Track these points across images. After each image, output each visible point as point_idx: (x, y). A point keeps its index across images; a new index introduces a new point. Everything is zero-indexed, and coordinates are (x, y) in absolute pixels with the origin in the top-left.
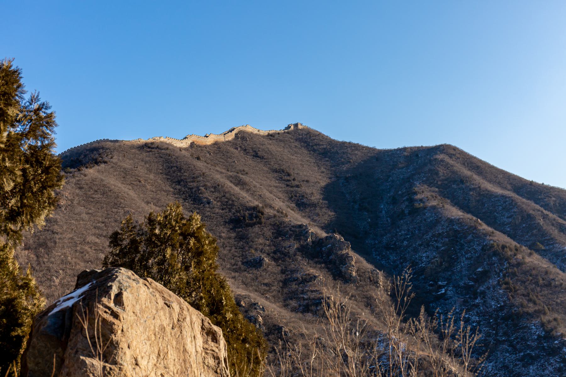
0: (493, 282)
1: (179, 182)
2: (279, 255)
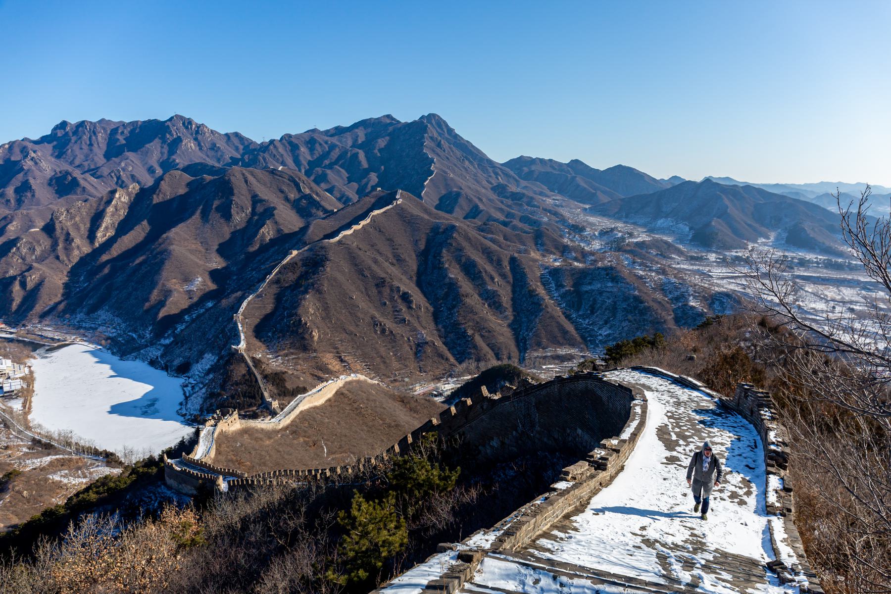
0: (455, 310)
1: (356, 265)
2: (392, 299)
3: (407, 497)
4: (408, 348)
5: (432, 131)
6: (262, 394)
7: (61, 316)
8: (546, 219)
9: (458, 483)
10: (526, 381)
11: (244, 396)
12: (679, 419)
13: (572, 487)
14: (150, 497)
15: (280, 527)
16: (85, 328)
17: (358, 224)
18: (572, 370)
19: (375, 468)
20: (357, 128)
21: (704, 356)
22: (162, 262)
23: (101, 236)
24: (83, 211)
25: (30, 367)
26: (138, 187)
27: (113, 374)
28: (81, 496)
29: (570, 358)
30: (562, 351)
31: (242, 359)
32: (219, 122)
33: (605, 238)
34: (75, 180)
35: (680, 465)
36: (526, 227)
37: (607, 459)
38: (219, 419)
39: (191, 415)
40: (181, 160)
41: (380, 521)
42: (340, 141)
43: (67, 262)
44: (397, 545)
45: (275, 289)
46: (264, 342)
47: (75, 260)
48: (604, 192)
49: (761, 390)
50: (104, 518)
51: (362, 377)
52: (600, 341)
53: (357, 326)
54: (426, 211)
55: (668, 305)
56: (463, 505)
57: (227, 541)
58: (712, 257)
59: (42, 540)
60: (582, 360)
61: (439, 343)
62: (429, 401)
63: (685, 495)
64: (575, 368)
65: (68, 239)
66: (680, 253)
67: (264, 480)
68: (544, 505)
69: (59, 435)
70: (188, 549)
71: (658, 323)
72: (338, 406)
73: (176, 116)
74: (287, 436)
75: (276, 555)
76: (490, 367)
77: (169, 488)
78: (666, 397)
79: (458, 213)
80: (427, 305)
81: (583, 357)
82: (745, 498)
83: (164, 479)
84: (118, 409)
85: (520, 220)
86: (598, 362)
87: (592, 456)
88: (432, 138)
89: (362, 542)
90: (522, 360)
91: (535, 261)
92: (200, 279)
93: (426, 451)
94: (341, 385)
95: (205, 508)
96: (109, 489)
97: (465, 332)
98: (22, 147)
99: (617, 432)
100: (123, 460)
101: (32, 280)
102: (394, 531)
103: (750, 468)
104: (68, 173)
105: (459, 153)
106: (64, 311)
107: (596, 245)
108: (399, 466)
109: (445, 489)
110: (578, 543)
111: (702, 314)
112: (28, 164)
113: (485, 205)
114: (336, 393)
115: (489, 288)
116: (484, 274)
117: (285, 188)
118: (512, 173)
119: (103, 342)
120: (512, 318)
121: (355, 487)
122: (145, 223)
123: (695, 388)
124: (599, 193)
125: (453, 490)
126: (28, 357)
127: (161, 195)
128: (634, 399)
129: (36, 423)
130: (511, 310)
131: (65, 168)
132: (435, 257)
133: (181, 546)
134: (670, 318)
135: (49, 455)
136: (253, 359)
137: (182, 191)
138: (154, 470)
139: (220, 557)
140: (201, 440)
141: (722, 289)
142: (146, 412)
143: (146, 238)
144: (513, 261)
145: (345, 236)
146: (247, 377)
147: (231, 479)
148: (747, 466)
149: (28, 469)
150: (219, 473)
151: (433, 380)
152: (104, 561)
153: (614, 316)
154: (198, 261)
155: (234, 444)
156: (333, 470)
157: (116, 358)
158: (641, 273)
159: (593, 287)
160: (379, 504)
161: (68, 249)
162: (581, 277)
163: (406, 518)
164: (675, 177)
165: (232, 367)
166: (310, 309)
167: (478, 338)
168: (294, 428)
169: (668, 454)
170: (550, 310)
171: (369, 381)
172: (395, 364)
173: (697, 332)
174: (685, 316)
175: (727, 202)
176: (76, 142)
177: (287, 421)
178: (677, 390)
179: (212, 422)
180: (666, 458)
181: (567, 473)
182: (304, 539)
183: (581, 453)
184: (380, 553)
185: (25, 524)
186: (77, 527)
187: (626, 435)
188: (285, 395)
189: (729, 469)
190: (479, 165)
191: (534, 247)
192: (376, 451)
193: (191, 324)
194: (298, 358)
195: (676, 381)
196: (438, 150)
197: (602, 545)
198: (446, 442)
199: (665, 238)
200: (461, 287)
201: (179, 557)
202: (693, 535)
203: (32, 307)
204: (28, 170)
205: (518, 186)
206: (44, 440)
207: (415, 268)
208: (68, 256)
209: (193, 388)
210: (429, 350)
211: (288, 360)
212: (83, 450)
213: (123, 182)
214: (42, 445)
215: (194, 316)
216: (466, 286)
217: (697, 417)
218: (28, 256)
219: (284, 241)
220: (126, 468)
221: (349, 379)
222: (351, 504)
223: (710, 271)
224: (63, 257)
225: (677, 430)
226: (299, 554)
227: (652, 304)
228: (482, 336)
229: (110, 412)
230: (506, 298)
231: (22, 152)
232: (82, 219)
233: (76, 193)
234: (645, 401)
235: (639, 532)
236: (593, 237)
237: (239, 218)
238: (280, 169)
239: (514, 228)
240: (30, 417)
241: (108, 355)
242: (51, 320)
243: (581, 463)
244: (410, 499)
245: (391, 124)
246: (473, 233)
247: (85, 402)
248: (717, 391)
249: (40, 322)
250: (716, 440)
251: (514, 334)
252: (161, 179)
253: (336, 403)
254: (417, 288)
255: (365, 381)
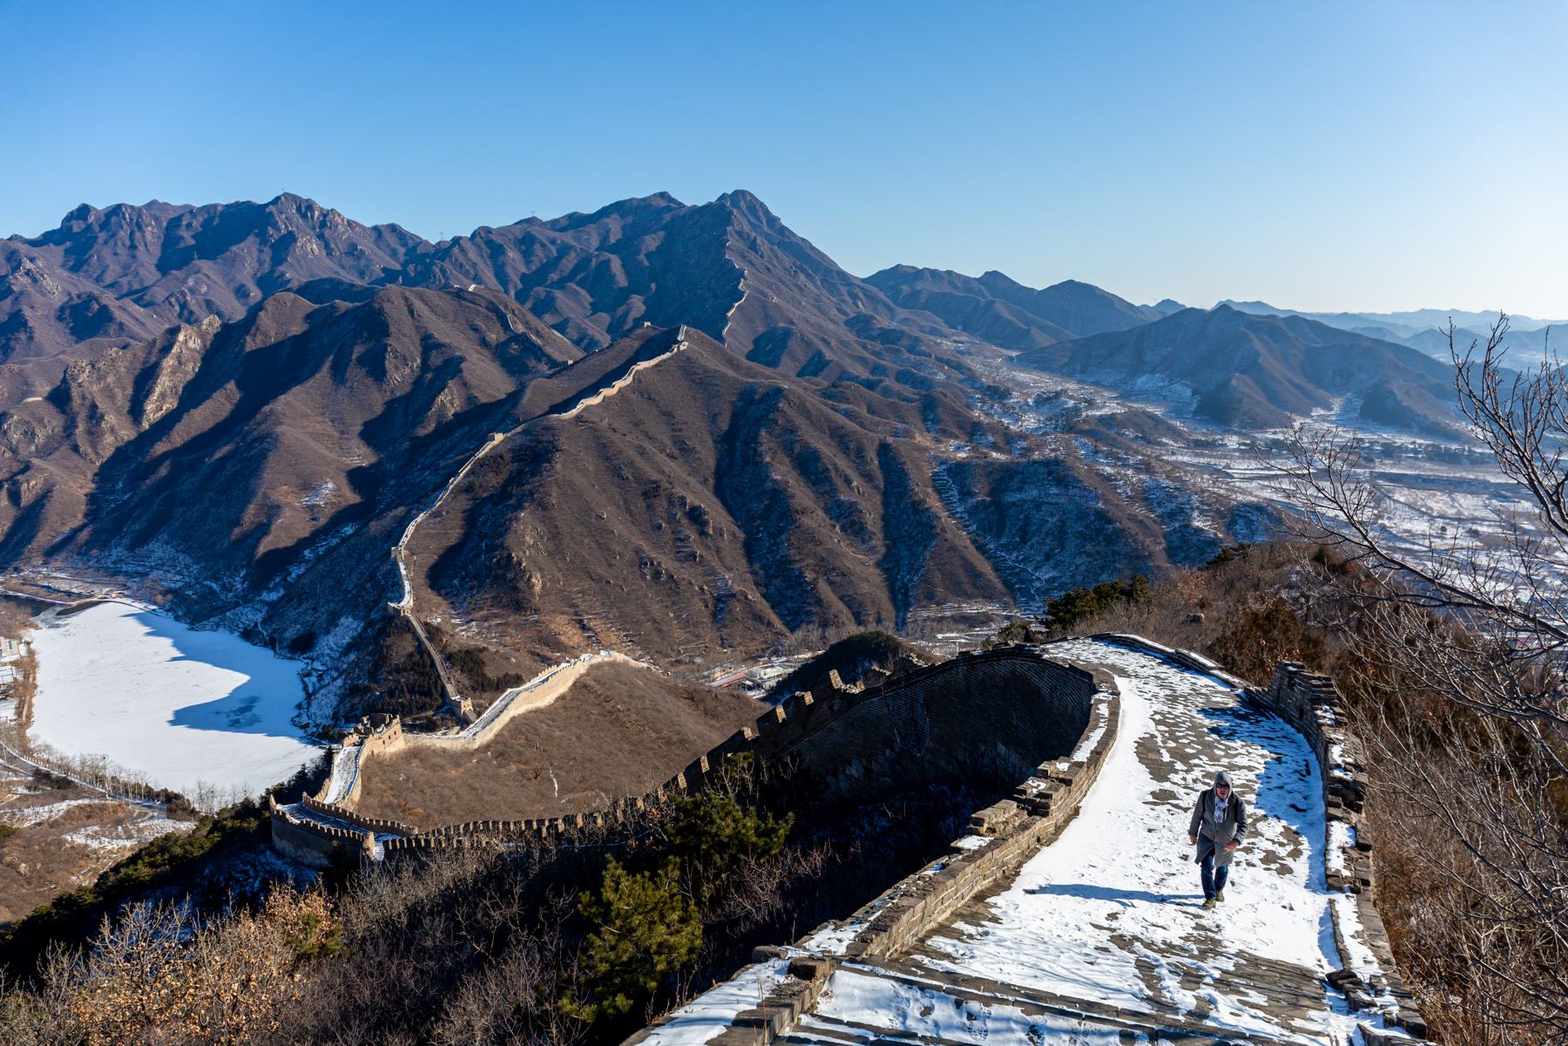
0: (783, 537)
2: (671, 518)
3: (700, 867)
4: (700, 605)
5: (741, 221)
6: (443, 688)
7: (83, 551)
8: (941, 377)
9: (790, 841)
10: (907, 661)
11: (412, 692)
12: (1176, 725)
13: (989, 845)
14: (246, 872)
15: (477, 921)
16: (126, 573)
17: (609, 385)
18: (988, 641)
19: (643, 815)
20: (608, 215)
21: (1218, 615)
22: (263, 456)
23: (153, 410)
24: (120, 365)
25: (28, 643)
26: (217, 322)
27: (178, 654)
28: (123, 870)
29: (984, 620)
30: (971, 609)
31: (407, 626)
32: (362, 207)
33: (1045, 409)
34: (104, 309)
35: (1177, 806)
36: (907, 391)
37: (1050, 796)
38: (367, 733)
39: (317, 726)
40: (294, 275)
41: (653, 909)
42: (578, 240)
43: (92, 456)
44: (683, 951)
45: (464, 503)
46: (446, 596)
47: (107, 453)
48: (1043, 329)
49: (1317, 674)
50: (164, 910)
51: (620, 657)
52: (1038, 589)
53: (610, 566)
54: (731, 362)
55: (1156, 527)
56: (799, 878)
57: (383, 947)
58: (1232, 442)
59: (54, 949)
60: (1006, 624)
61: (754, 596)
62: (738, 697)
63: (1185, 858)
64: (994, 638)
65: (94, 415)
66: (1176, 434)
67: (449, 839)
68: (940, 878)
69: (83, 763)
70: (313, 962)
71: (1138, 558)
72: (577, 708)
73: (285, 195)
74: (489, 762)
75: (471, 971)
76: (845, 636)
77: (280, 855)
78: (1152, 687)
79: (788, 366)
80: (735, 528)
81: (1007, 618)
82: (1289, 862)
83: (270, 840)
84: (188, 717)
85: (897, 379)
86: (1034, 628)
87: (1024, 792)
88: (740, 234)
89: (622, 946)
90: (901, 624)
91: (926, 449)
92: (330, 485)
93: (734, 785)
94: (583, 671)
95: (344, 889)
96: (173, 858)
97: (801, 576)
98: (12, 252)
99: (1067, 750)
100: (197, 806)
101: (30, 488)
102: (678, 926)
103: (1299, 810)
104: (92, 297)
105: (787, 260)
106: (89, 544)
107: (1030, 422)
108: (686, 812)
109: (767, 851)
110: (1000, 942)
111: (1214, 542)
112: (20, 281)
113: (834, 352)
114: (574, 684)
115: (842, 497)
116: (833, 474)
117: (479, 323)
118: (881, 295)
119: (159, 598)
120: (883, 550)
121: (608, 850)
122: (231, 385)
123: (1202, 670)
124: (1034, 331)
125: (781, 853)
126: (25, 625)
127: (259, 337)
128: (1097, 692)
129: (40, 742)
130: (881, 536)
131: (88, 290)
132: (746, 443)
133: (302, 958)
134: (1159, 548)
135: (64, 798)
136: (427, 626)
137: (297, 329)
138: (253, 824)
139: (372, 975)
140: (335, 770)
141: (1250, 498)
142: (237, 721)
143: (233, 412)
144: (884, 449)
145: (587, 408)
146: (417, 658)
147: (390, 838)
148: (1293, 806)
149: (27, 824)
150: (368, 827)
151: (745, 660)
152: (165, 985)
153: (1062, 546)
154: (326, 453)
155: (394, 777)
156: (570, 820)
157: (182, 627)
158: (1109, 470)
159: (1024, 496)
160: (651, 879)
161: (94, 434)
162: (1004, 477)
163: (699, 903)
164: (1167, 302)
165: (389, 641)
166: (526, 537)
167: (823, 587)
168: (501, 748)
169: (1156, 786)
170: (949, 536)
171: (633, 663)
172: (678, 634)
173: (1205, 574)
174: (1185, 547)
175: (1258, 345)
176: (106, 242)
177: (487, 736)
178: (1172, 675)
179: (355, 738)
180: (1153, 793)
181: (980, 822)
182: (519, 942)
183: (1006, 788)
184: (653, 965)
185: (24, 922)
186: (117, 925)
187: (1082, 754)
188: (484, 690)
189: (1261, 812)
190: (823, 281)
191: (920, 425)
192: (647, 786)
193: (315, 565)
194: (506, 624)
195: (1168, 660)
196: (751, 255)
197: (1042, 947)
198: (769, 769)
199: (1150, 409)
200: (793, 497)
201: (298, 976)
202: (1199, 927)
203: (30, 538)
204: (21, 293)
205: (892, 319)
206: (55, 773)
207: (711, 462)
208: (94, 445)
209: (320, 678)
210: (738, 608)
211: (489, 628)
212: (125, 790)
213: (191, 313)
214: (53, 782)
215: (321, 551)
216: (801, 494)
217: (1207, 722)
218: (22, 445)
219: (481, 417)
220: (203, 820)
221: (597, 659)
222: (602, 879)
223: (1228, 466)
224: (85, 447)
225: (1172, 744)
226: (510, 969)
227: (1127, 524)
228: (831, 583)
229: (173, 723)
230: (871, 515)
231: (9, 260)
232: (119, 379)
233: (106, 334)
234: (1116, 693)
235: (1106, 924)
236: (1025, 408)
237: (400, 377)
238: (471, 289)
239: (886, 392)
240: (29, 732)
241: (168, 621)
242: (66, 559)
243: (1003, 803)
244: (705, 870)
245: (668, 209)
246: (814, 402)
247: (132, 706)
248: (1241, 676)
249: (45, 563)
250: (1239, 761)
251: (887, 580)
252: (259, 307)
253: (575, 703)
254: (715, 499)
255: (626, 664)
